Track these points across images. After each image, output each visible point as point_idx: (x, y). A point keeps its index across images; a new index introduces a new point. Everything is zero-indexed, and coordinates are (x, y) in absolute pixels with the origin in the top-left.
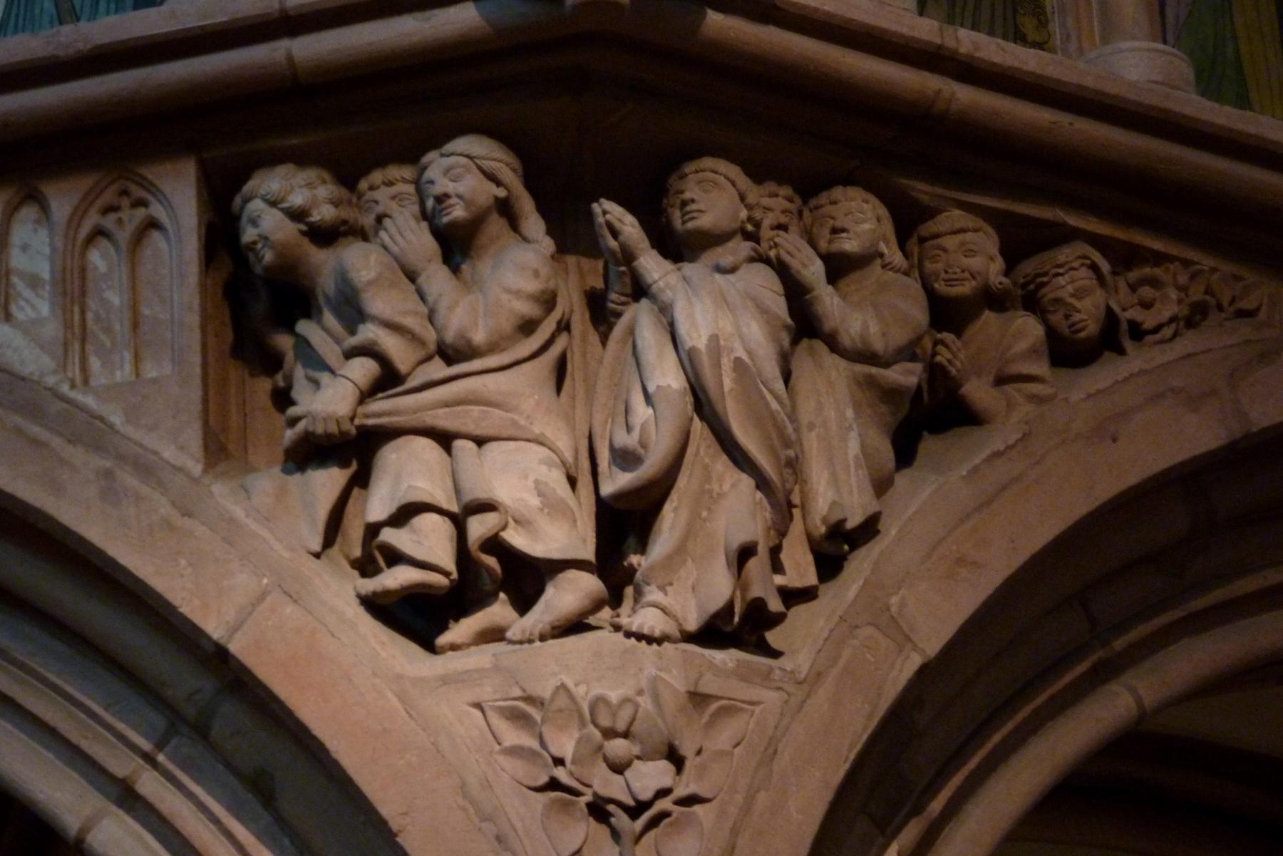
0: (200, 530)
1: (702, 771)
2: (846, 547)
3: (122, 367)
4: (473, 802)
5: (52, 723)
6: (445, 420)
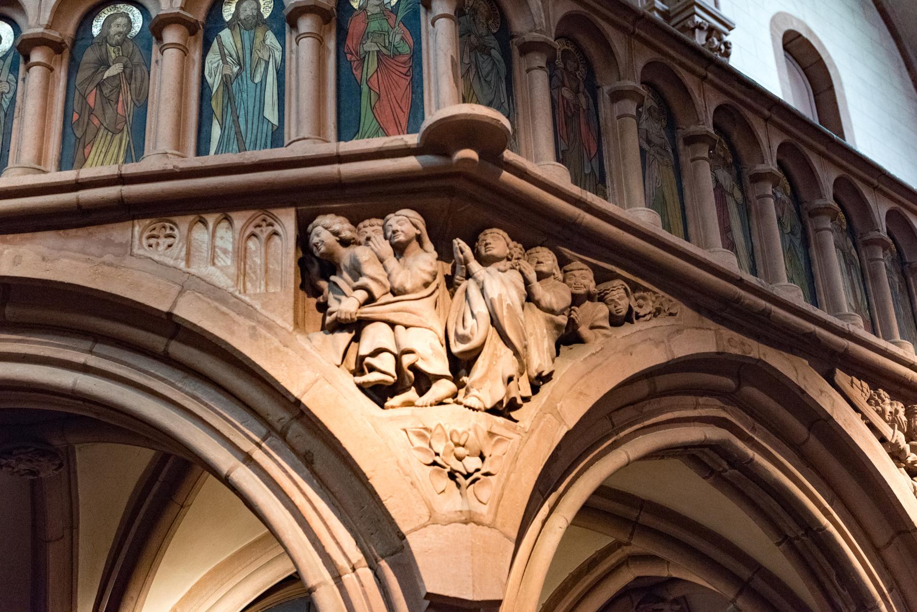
0: (291, 352)
1: (492, 462)
2: (541, 383)
3: (260, 288)
4: (402, 468)
5: (218, 428)
6: (393, 317)
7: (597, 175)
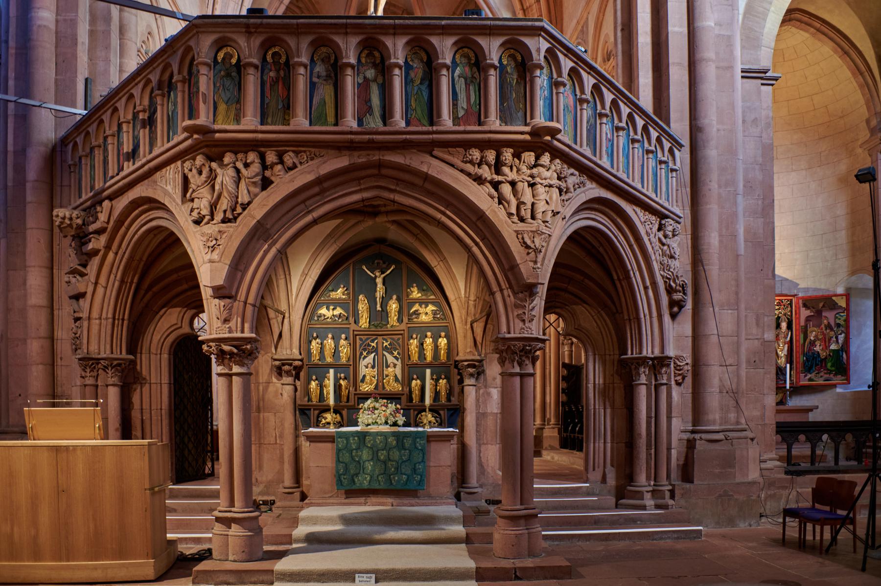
6: (198, 196)
7: (286, 106)
